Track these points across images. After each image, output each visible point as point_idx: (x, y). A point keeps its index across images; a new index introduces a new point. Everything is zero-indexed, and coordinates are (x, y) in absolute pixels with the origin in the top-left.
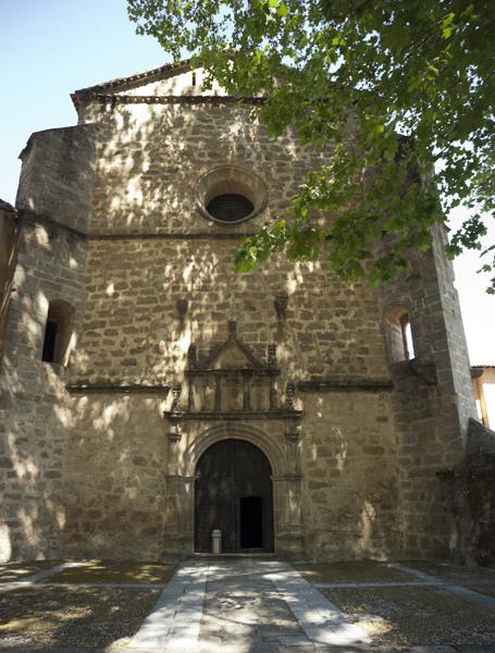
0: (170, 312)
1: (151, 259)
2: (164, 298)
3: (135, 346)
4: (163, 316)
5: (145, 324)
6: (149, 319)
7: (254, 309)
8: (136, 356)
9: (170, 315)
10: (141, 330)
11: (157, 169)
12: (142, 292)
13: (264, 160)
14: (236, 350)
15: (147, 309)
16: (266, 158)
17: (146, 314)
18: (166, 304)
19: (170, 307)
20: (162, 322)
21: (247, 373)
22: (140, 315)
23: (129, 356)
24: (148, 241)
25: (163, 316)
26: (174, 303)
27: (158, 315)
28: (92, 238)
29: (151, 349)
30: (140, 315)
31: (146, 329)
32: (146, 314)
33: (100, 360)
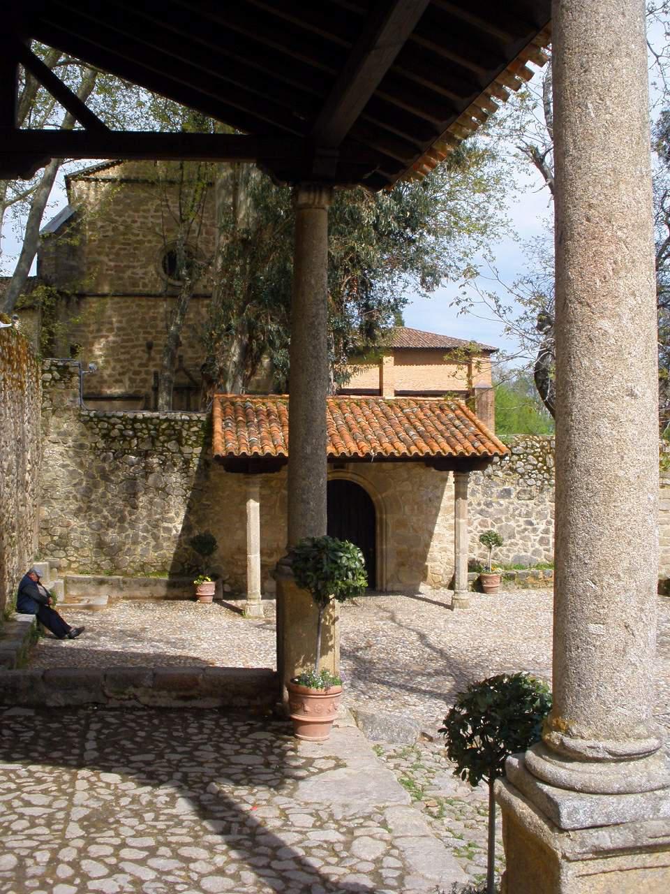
0: (142, 348)
1: (129, 311)
2: (137, 339)
3: (121, 370)
4: (138, 352)
5: (127, 356)
6: (128, 353)
7: (193, 347)
8: (122, 377)
9: (143, 351)
10: (125, 360)
11: (130, 242)
12: (124, 335)
13: (204, 235)
14: (182, 373)
15: (127, 347)
16: (206, 233)
17: (127, 349)
18: (139, 343)
19: (141, 346)
20: (137, 355)
21: (189, 388)
22: (123, 350)
23: (118, 377)
24: (126, 298)
25: (138, 352)
26: (145, 343)
27: (135, 350)
28: (89, 296)
29: (131, 373)
30: (123, 350)
31: (128, 360)
32: (127, 349)
33: (100, 380)
